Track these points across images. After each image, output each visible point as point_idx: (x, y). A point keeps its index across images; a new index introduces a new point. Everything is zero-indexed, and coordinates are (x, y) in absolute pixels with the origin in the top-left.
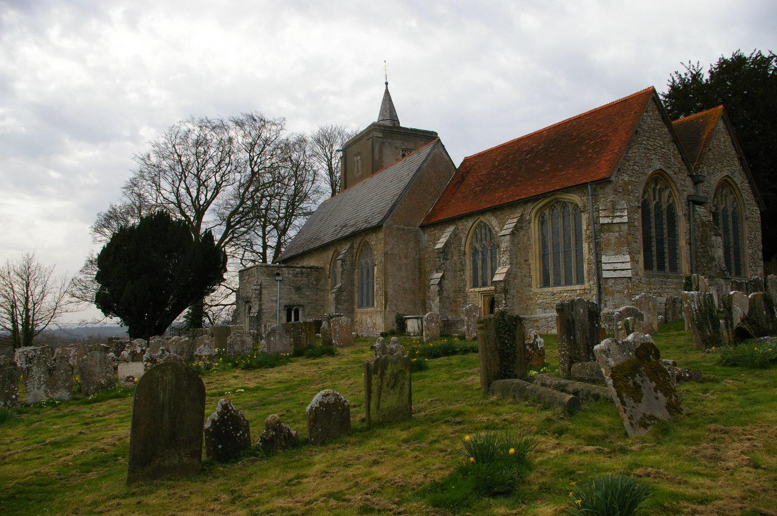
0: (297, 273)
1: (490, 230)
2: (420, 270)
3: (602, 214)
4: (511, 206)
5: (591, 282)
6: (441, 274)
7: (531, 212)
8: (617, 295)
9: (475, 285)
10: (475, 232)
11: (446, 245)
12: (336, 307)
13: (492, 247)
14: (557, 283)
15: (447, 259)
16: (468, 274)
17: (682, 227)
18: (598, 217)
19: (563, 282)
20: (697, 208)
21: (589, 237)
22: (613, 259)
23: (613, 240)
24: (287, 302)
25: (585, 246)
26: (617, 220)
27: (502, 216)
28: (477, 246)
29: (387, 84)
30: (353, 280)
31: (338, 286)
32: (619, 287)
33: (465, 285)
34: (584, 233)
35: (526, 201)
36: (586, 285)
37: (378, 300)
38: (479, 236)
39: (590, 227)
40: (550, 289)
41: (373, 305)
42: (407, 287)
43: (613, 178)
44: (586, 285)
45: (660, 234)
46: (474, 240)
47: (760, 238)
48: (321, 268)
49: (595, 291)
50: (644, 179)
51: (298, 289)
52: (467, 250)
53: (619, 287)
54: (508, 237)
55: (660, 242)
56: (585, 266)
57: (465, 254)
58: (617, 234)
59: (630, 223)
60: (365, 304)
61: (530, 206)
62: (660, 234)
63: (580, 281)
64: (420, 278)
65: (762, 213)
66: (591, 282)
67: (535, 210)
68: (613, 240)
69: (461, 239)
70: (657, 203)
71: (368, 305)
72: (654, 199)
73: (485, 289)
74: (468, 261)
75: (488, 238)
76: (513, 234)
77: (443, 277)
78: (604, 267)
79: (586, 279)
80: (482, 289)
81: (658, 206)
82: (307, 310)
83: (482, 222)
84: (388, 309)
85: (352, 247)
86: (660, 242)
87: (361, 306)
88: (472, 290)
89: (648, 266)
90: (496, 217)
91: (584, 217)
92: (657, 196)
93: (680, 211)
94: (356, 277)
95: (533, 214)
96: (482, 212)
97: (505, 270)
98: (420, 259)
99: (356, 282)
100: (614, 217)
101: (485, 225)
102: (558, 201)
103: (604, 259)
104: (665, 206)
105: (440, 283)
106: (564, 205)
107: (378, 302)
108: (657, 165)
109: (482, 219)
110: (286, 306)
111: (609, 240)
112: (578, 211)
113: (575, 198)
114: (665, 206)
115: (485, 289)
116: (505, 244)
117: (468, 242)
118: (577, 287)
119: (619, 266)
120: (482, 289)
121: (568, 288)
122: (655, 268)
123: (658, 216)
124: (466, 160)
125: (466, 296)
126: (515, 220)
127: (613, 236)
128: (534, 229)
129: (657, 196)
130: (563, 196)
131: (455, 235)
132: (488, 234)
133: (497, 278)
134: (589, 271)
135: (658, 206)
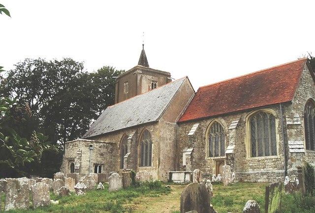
0: (101, 146)
1: (220, 126)
3: (287, 119)
4: (234, 114)
5: (281, 155)
6: (191, 150)
7: (246, 118)
8: (297, 162)
9: (211, 156)
10: (211, 127)
12: (127, 166)
13: (221, 135)
14: (260, 155)
15: (195, 141)
16: (206, 150)
18: (286, 121)
19: (270, 153)
21: (280, 131)
23: (294, 133)
24: (95, 162)
25: (278, 136)
26: (296, 123)
29: (143, 45)
30: (137, 151)
31: (128, 154)
32: (298, 158)
33: (205, 156)
34: (277, 129)
35: (242, 112)
36: (278, 156)
37: (155, 162)
38: (213, 129)
39: (280, 126)
40: (257, 158)
41: (150, 165)
43: (293, 102)
44: (278, 156)
46: (211, 131)
48: (114, 144)
49: (283, 158)
50: (304, 103)
51: (102, 155)
52: (206, 137)
53: (298, 158)
54: (234, 130)
56: (278, 147)
57: (205, 139)
58: (296, 130)
60: (144, 165)
61: (245, 115)
63: (274, 153)
66: (281, 155)
68: (294, 133)
69: (202, 130)
71: (146, 165)
73: (217, 158)
74: (206, 142)
76: (236, 128)
77: (193, 151)
79: (278, 154)
80: (215, 158)
81: (310, 116)
82: (106, 166)
83: (216, 122)
84: (160, 168)
85: (137, 133)
87: (141, 165)
88: (209, 158)
89: (307, 148)
91: (277, 121)
94: (139, 149)
95: (247, 119)
96: (217, 117)
99: (139, 153)
102: (261, 112)
103: (289, 142)
105: (191, 154)
106: (265, 114)
107: (153, 163)
108: (309, 96)
109: (216, 120)
110: (94, 164)
111: (292, 133)
112: (272, 118)
113: (273, 111)
115: (217, 158)
116: (232, 134)
117: (207, 131)
120: (215, 158)
121: (268, 157)
124: (200, 89)
125: (205, 162)
128: (248, 126)
130: (264, 110)
131: (199, 128)
132: (219, 128)
134: (279, 149)
135: (310, 116)
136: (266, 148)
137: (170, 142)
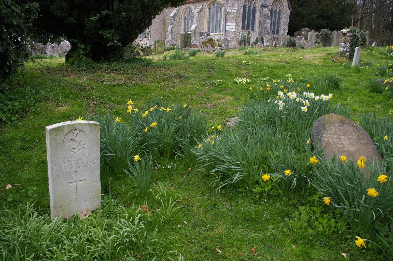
1: (191, 10)
2: (164, 24)
3: (229, 8)
6: (172, 26)
7: (206, 4)
11: (175, 15)
15: (174, 21)
17: (258, 15)
20: (264, 8)
22: (230, 24)
25: (222, 19)
26: (233, 11)
27: (196, 5)
28: (186, 16)
33: (181, 31)
38: (187, 12)
42: (159, 30)
44: (221, 33)
45: (249, 17)
46: (185, 14)
47: (288, 22)
53: (231, 34)
54: (197, 14)
55: (249, 20)
56: (222, 26)
59: (238, 12)
62: (249, 17)
63: (220, 32)
64: (164, 27)
65: (290, 12)
67: (207, 4)
68: (231, 18)
69: (180, 13)
70: (250, 6)
72: (249, 4)
74: (182, 22)
75: (190, 13)
76: (199, 12)
77: (172, 27)
78: (227, 27)
79: (221, 31)
81: (250, 7)
86: (249, 20)
89: (243, 28)
90: (194, 5)
91: (223, 8)
92: (250, 3)
93: (258, 9)
95: (207, 6)
97: (195, 26)
98: (164, 20)
100: (232, 9)
101: (190, 8)
103: (227, 24)
104: (252, 7)
105: (171, 29)
114: (252, 7)
116: (196, 16)
118: (219, 34)
119: (232, 27)
121: (216, 34)
122: (246, 29)
123: (249, 10)
126: (200, 7)
127: (230, 16)
128: (206, 11)
129: (250, 3)
131: (178, 11)
132: (190, 12)
133: (192, 29)
134: (223, 28)
136: (216, 28)
137: (158, 20)
